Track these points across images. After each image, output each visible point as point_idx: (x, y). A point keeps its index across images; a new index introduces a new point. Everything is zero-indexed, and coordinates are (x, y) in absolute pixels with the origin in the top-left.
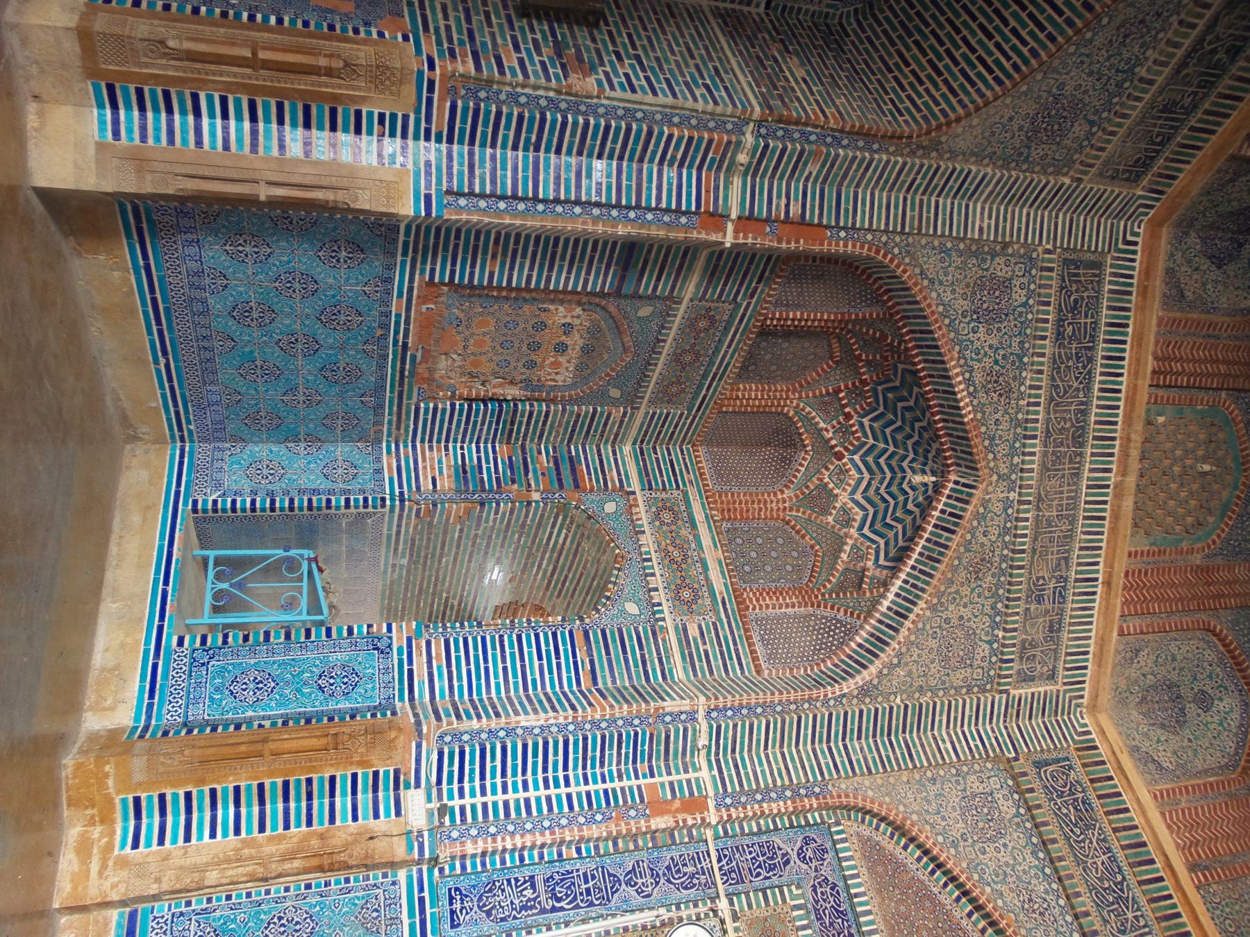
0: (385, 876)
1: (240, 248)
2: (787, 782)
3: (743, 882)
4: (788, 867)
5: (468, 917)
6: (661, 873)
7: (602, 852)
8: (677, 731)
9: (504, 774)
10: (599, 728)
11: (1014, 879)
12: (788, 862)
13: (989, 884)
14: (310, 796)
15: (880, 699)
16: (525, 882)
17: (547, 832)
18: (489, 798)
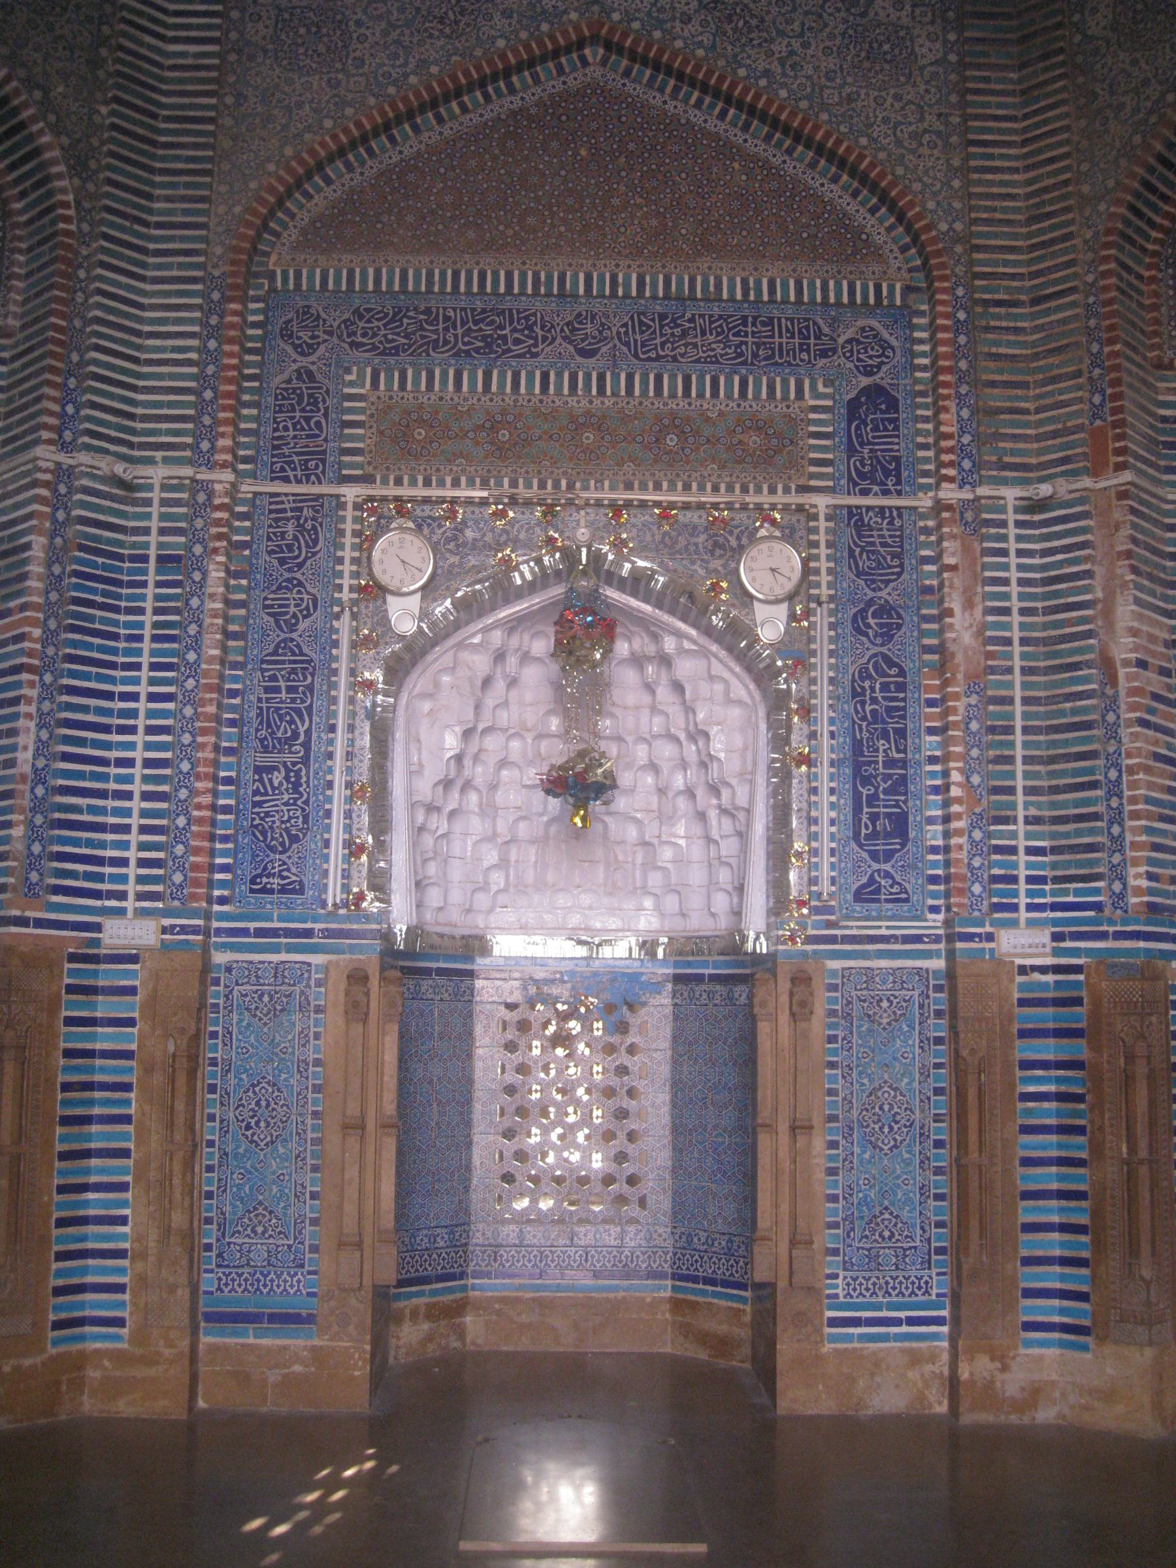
0: (216, 982)
2: (195, 343)
3: (324, 452)
4: (319, 377)
5: (294, 870)
6: (287, 575)
7: (240, 659)
8: (83, 505)
9: (103, 794)
10: (56, 633)
11: (407, 32)
12: (310, 375)
13: (406, 75)
14: (89, 1086)
15: (95, 142)
16: (261, 780)
17: (200, 739)
18: (135, 821)
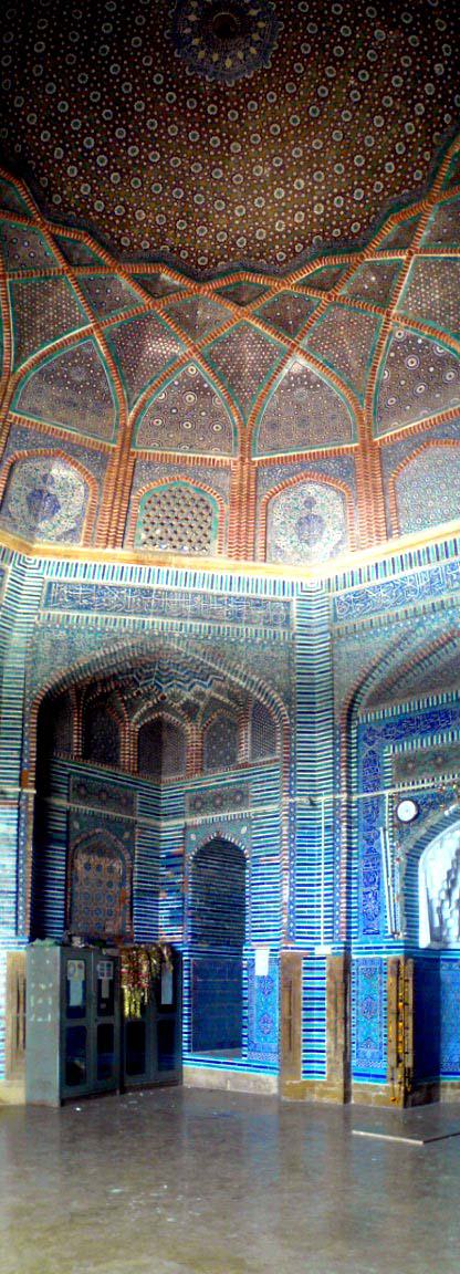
9: (312, 906)
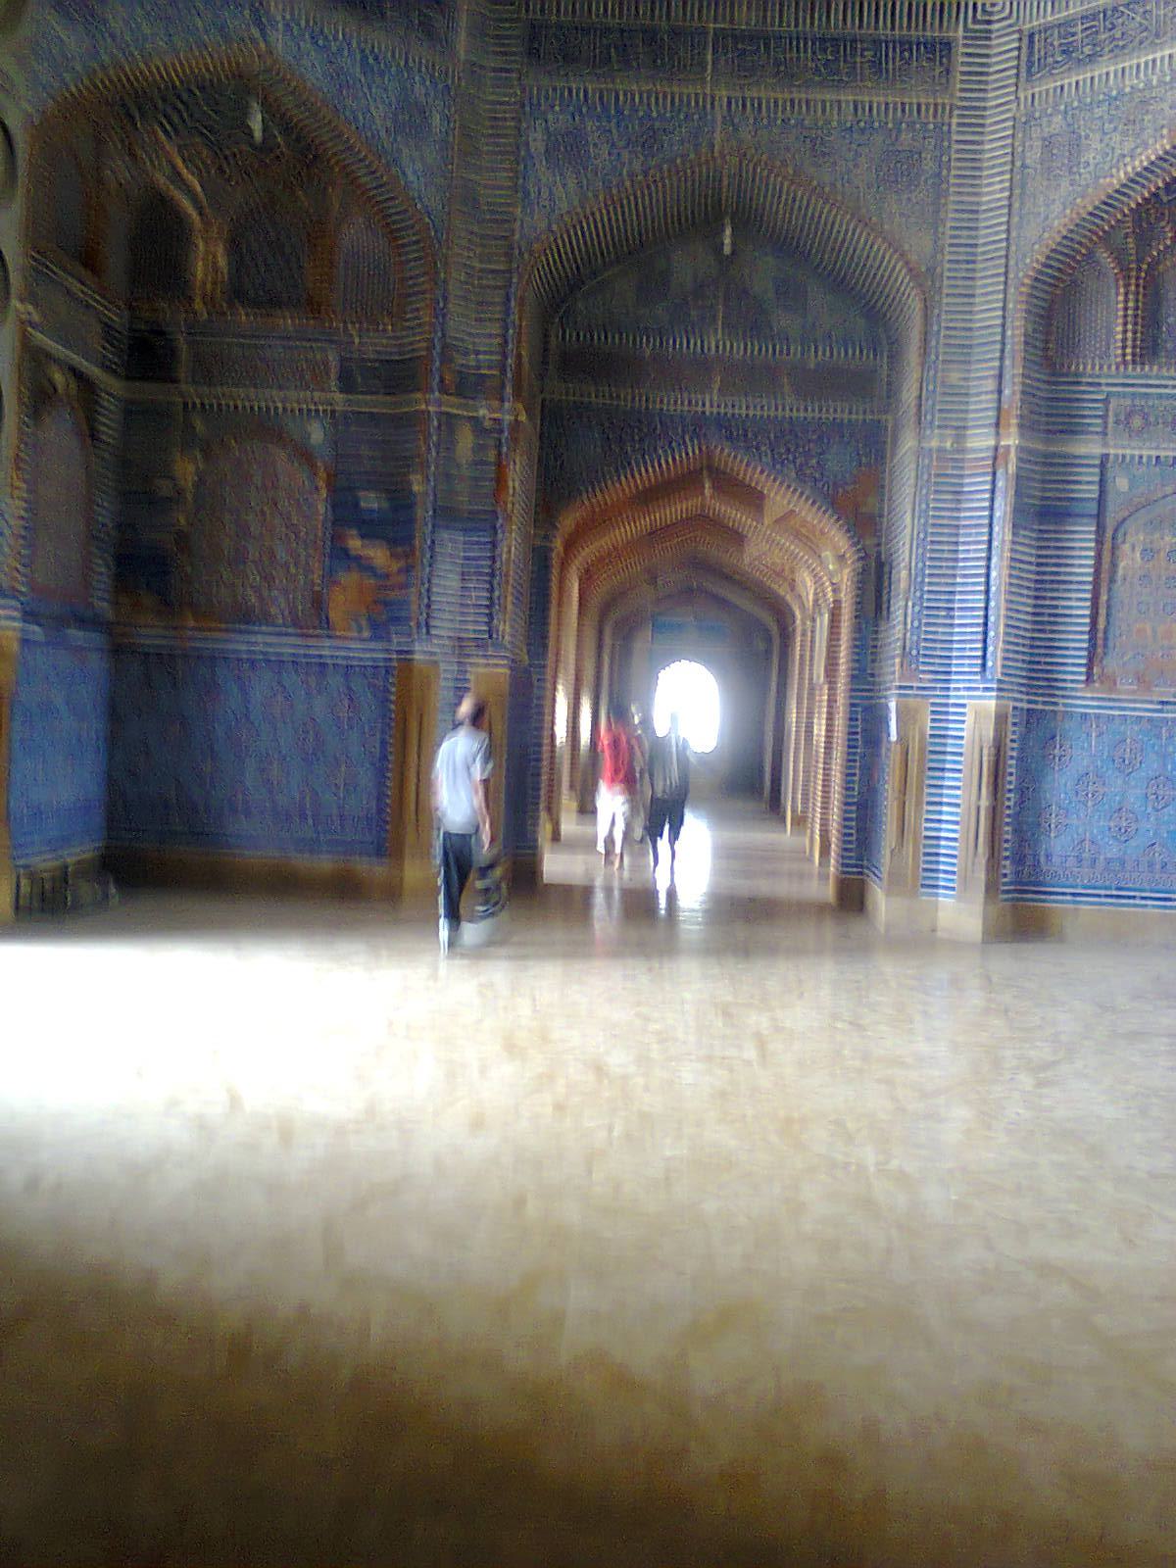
1: (1053, 826)
